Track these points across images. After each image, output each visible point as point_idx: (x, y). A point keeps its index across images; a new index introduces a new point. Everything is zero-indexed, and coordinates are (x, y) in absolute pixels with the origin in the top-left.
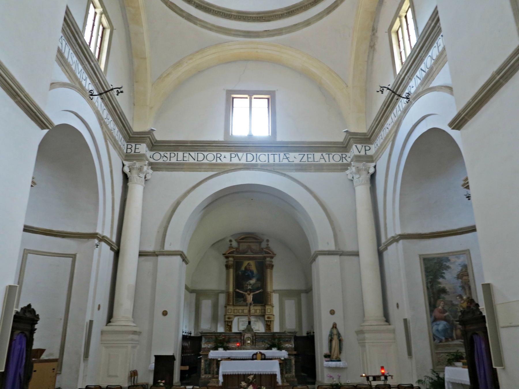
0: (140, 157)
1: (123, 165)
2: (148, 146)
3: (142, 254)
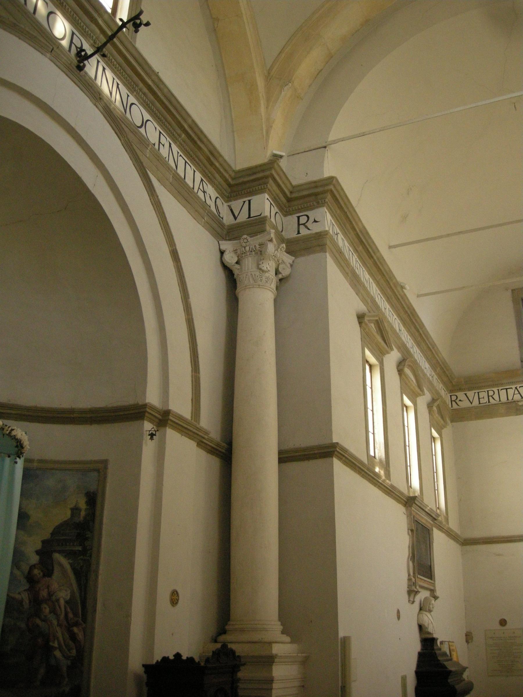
0: (257, 225)
1: (222, 253)
2: (275, 200)
3: (285, 457)
